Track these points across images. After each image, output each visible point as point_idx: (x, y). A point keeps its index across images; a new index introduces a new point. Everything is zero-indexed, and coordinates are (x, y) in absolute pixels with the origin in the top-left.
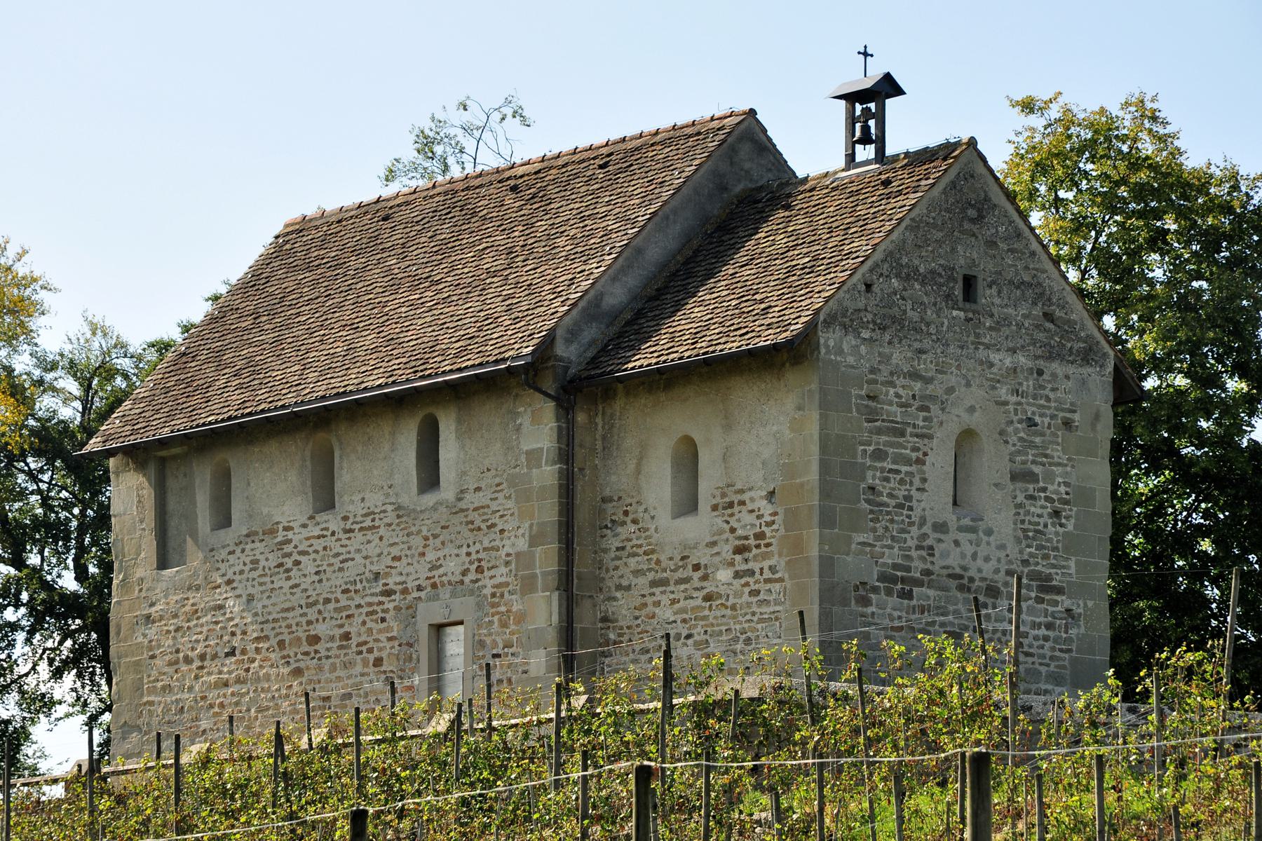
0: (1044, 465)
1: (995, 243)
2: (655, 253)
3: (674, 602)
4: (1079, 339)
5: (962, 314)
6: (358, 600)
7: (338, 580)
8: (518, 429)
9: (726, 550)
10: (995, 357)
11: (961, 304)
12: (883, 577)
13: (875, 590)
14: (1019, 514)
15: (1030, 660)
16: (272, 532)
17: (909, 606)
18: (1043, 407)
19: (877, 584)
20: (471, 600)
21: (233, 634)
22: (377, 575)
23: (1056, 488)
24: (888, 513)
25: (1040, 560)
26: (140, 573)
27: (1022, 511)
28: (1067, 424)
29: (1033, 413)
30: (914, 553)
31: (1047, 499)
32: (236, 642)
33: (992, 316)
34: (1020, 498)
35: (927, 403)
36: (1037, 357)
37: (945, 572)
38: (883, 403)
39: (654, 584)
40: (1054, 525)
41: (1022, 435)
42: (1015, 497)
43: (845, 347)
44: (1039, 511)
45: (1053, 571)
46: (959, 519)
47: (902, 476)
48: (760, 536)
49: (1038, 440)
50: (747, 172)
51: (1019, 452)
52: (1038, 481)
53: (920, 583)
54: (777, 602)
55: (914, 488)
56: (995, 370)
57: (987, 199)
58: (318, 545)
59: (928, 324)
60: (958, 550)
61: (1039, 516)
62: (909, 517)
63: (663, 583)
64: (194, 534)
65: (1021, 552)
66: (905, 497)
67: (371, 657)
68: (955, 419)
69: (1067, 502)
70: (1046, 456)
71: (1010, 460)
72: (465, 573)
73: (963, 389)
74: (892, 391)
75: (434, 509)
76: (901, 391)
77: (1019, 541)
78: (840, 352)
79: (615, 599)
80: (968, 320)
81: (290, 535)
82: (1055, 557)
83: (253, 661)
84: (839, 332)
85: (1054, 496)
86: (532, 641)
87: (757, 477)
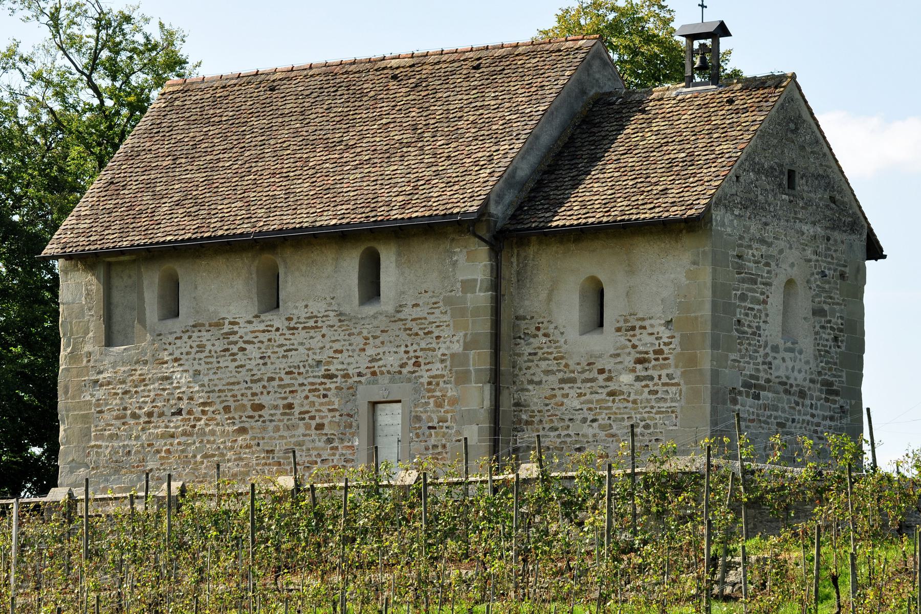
1: (804, 147)
2: (545, 140)
3: (580, 395)
4: (849, 215)
6: (301, 380)
7: (283, 364)
8: (455, 264)
9: (629, 361)
10: (805, 228)
11: (787, 190)
12: (746, 385)
13: (740, 393)
16: (219, 325)
17: (758, 404)
18: (829, 263)
19: (741, 389)
20: (408, 386)
21: (180, 399)
22: (319, 363)
24: (748, 339)
25: (827, 372)
26: (88, 348)
27: (818, 337)
28: (842, 276)
30: (761, 367)
31: (832, 328)
32: (183, 405)
33: (803, 199)
35: (769, 261)
36: (827, 228)
37: (777, 380)
38: (746, 261)
39: (562, 381)
41: (818, 283)
42: (814, 327)
43: (726, 220)
45: (834, 379)
46: (785, 343)
47: (755, 312)
48: (659, 352)
49: (827, 286)
50: (597, 81)
51: (817, 295)
52: (826, 316)
53: (763, 388)
54: (672, 400)
55: (761, 321)
56: (805, 237)
57: (800, 116)
58: (264, 337)
59: (769, 205)
60: (784, 364)
61: (827, 340)
62: (759, 341)
63: (573, 381)
64: (142, 321)
65: (817, 366)
67: (313, 423)
68: (784, 272)
69: (841, 330)
70: (831, 298)
72: (403, 366)
73: (788, 251)
74: (750, 252)
75: (375, 317)
76: (756, 253)
78: (723, 225)
79: (528, 390)
80: (791, 202)
81: (236, 328)
83: (199, 419)
84: (723, 211)
86: (467, 418)
87: (657, 310)
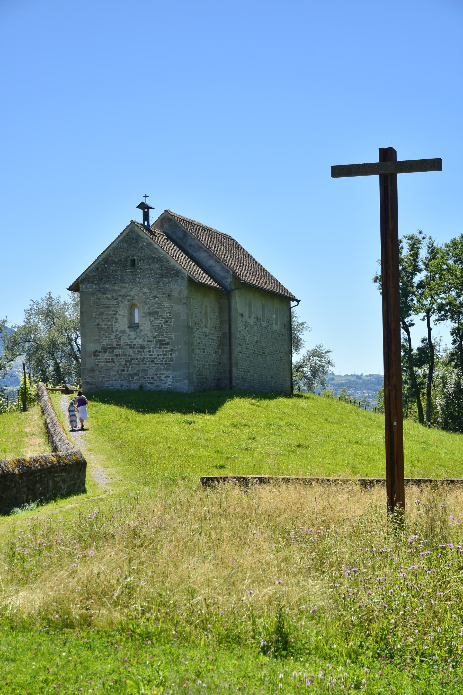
5: (130, 270)
12: (103, 348)
14: (152, 324)
15: (157, 365)
23: (166, 314)
24: (104, 330)
27: (153, 323)
29: (157, 294)
31: (163, 318)
34: (152, 319)
40: (165, 325)
41: (153, 301)
44: (159, 322)
52: (159, 313)
53: (117, 348)
61: (161, 323)
66: (110, 325)
69: (170, 318)
77: (152, 332)
78: (87, 288)
82: (166, 335)
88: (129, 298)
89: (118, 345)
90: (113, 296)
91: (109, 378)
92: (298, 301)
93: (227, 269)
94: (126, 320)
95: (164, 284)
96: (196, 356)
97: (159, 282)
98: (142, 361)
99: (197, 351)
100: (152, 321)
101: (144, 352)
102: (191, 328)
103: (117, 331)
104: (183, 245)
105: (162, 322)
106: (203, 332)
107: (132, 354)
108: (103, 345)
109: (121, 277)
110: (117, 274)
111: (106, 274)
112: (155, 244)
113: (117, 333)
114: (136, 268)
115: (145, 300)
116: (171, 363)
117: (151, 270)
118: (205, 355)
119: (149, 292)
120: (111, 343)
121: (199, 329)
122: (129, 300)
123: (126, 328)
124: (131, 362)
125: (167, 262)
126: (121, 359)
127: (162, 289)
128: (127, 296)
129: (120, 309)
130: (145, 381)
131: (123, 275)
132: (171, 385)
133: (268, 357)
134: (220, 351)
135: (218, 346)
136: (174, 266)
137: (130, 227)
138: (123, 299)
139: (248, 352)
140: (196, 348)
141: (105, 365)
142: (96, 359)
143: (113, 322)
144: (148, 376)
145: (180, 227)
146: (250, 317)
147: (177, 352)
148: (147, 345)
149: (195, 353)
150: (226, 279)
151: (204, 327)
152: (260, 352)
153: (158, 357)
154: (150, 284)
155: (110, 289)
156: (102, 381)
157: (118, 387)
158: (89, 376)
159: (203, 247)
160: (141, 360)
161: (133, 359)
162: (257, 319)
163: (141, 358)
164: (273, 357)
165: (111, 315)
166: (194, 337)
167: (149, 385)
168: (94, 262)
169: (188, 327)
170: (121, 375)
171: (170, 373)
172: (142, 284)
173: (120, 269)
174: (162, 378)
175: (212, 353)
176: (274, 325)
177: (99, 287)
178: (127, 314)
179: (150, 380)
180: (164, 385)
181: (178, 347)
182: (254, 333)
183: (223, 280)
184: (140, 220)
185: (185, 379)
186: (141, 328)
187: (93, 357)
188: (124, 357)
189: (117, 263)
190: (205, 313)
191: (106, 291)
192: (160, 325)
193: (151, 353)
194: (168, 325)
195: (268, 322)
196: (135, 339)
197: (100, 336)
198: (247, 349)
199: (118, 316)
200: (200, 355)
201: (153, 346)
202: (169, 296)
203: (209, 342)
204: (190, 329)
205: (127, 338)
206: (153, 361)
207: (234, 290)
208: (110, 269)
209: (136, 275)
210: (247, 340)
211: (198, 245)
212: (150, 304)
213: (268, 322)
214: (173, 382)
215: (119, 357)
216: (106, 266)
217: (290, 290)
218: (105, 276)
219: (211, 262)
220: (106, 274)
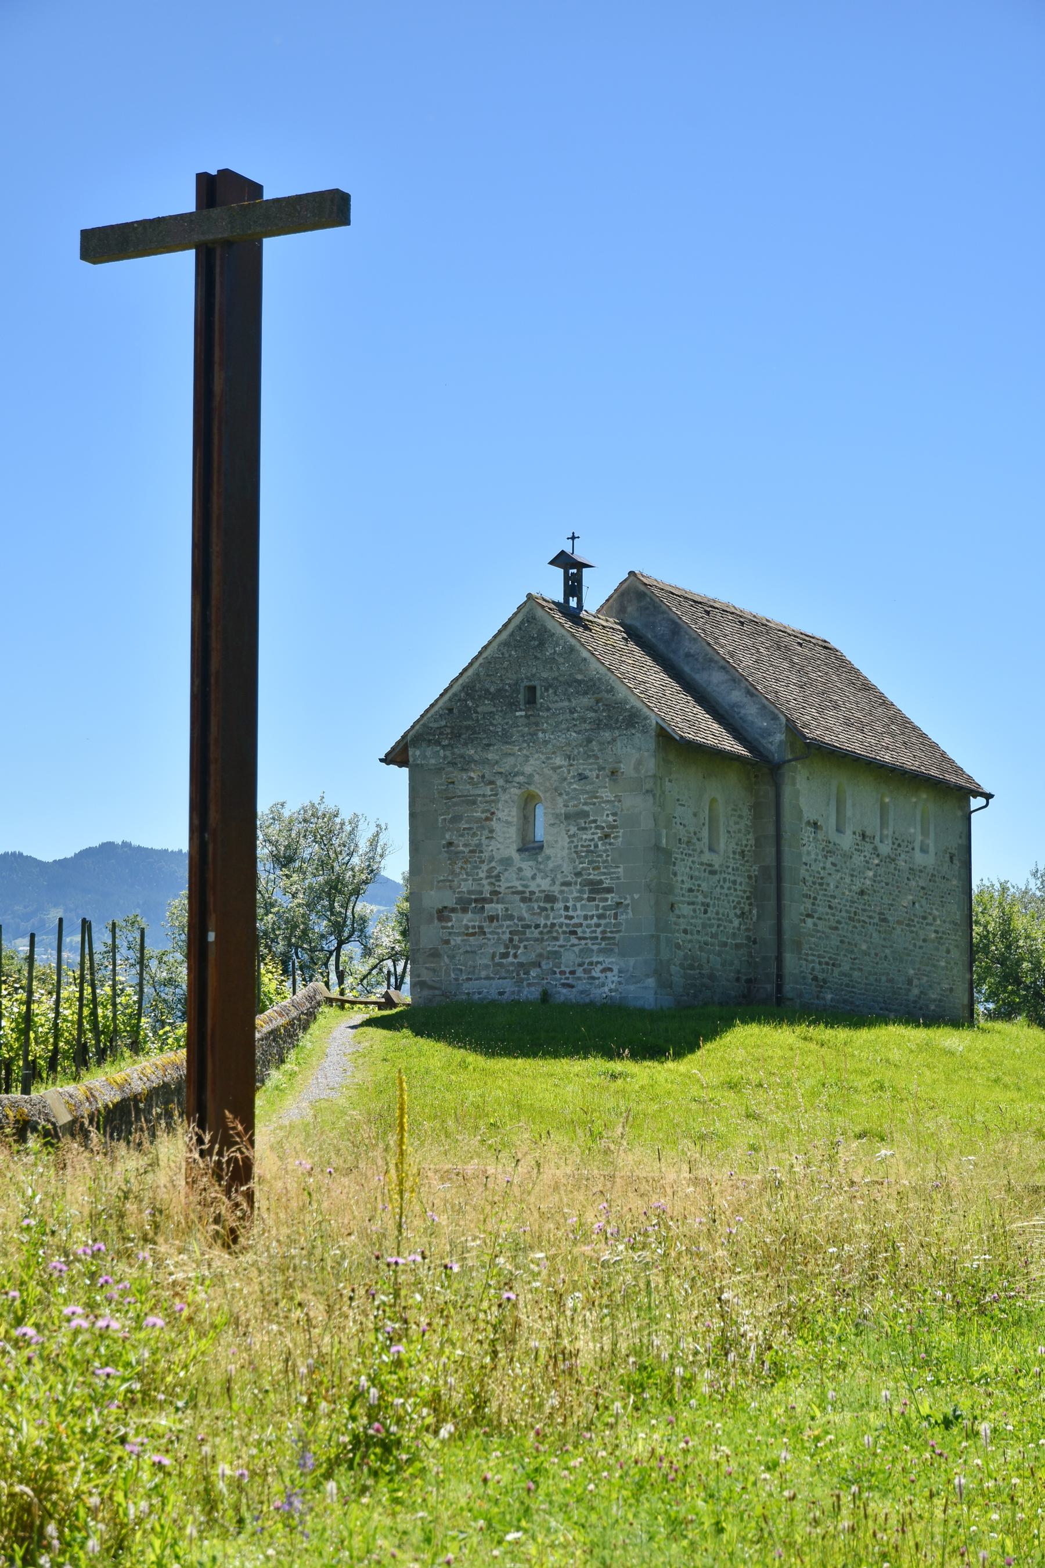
0: (594, 804)
5: (523, 713)
12: (460, 901)
14: (573, 842)
15: (583, 942)
23: (606, 818)
27: (575, 840)
29: (584, 769)
30: (485, 882)
31: (597, 827)
34: (573, 829)
40: (604, 844)
41: (575, 786)
44: (590, 837)
45: (603, 877)
49: (588, 788)
53: (491, 901)
61: (592, 840)
66: (477, 846)
71: (564, 806)
77: (573, 861)
78: (425, 757)
82: (605, 867)
85: (603, 825)
88: (520, 779)
89: (495, 893)
90: (483, 777)
91: (473, 973)
92: (988, 796)
93: (773, 713)
94: (513, 832)
95: (601, 744)
96: (682, 920)
97: (589, 741)
98: (549, 932)
99: (686, 910)
100: (574, 836)
101: (552, 909)
102: (668, 853)
103: (492, 859)
104: (671, 656)
105: (596, 837)
106: (702, 864)
107: (526, 915)
108: (459, 893)
109: (503, 729)
110: (495, 722)
111: (470, 723)
112: (582, 649)
113: (493, 864)
114: (539, 706)
115: (556, 784)
116: (617, 936)
117: (571, 712)
118: (709, 919)
119: (566, 764)
120: (478, 888)
121: (690, 855)
122: (520, 785)
123: (512, 852)
124: (524, 933)
125: (608, 691)
126: (502, 926)
127: (596, 757)
128: (516, 774)
129: (500, 805)
130: (556, 979)
131: (507, 724)
132: (616, 990)
133: (898, 931)
134: (754, 912)
135: (748, 898)
136: (626, 701)
137: (524, 610)
138: (507, 781)
139: (834, 915)
140: (683, 902)
141: (463, 941)
142: (443, 928)
143: (484, 838)
144: (563, 968)
145: (664, 612)
146: (839, 830)
147: (630, 911)
148: (562, 892)
149: (677, 912)
150: (769, 735)
151: (706, 850)
152: (870, 917)
153: (585, 923)
154: (568, 744)
155: (477, 757)
156: (456, 979)
157: (494, 994)
158: (427, 968)
159: (717, 658)
160: (545, 930)
161: (529, 927)
162: (864, 836)
163: (545, 926)
164: (912, 932)
165: (479, 820)
166: (675, 874)
167: (564, 991)
168: (442, 695)
169: (657, 848)
170: (501, 965)
171: (614, 960)
172: (550, 746)
173: (501, 711)
174: (594, 974)
175: (732, 915)
176: (918, 855)
177: (453, 754)
178: (515, 819)
179: (567, 978)
180: (598, 991)
181: (632, 899)
182: (853, 870)
183: (763, 737)
184: (557, 594)
185: (648, 976)
186: (547, 851)
187: (436, 921)
188: (508, 922)
189: (493, 697)
190: (710, 818)
191: (469, 762)
192: (592, 844)
193: (571, 913)
194: (610, 844)
195: (899, 845)
196: (534, 878)
197: (453, 872)
198: (830, 907)
199: (494, 824)
200: (693, 917)
201: (576, 894)
202: (613, 773)
203: (722, 887)
204: (662, 856)
205: (515, 876)
206: (574, 933)
207: (790, 761)
208: (479, 710)
209: (537, 724)
210: (832, 887)
211: (706, 655)
212: (568, 794)
213: (899, 845)
214: (620, 983)
215: (495, 923)
216: (470, 703)
217: (968, 770)
218: (468, 728)
219: (736, 696)
220: (470, 723)
